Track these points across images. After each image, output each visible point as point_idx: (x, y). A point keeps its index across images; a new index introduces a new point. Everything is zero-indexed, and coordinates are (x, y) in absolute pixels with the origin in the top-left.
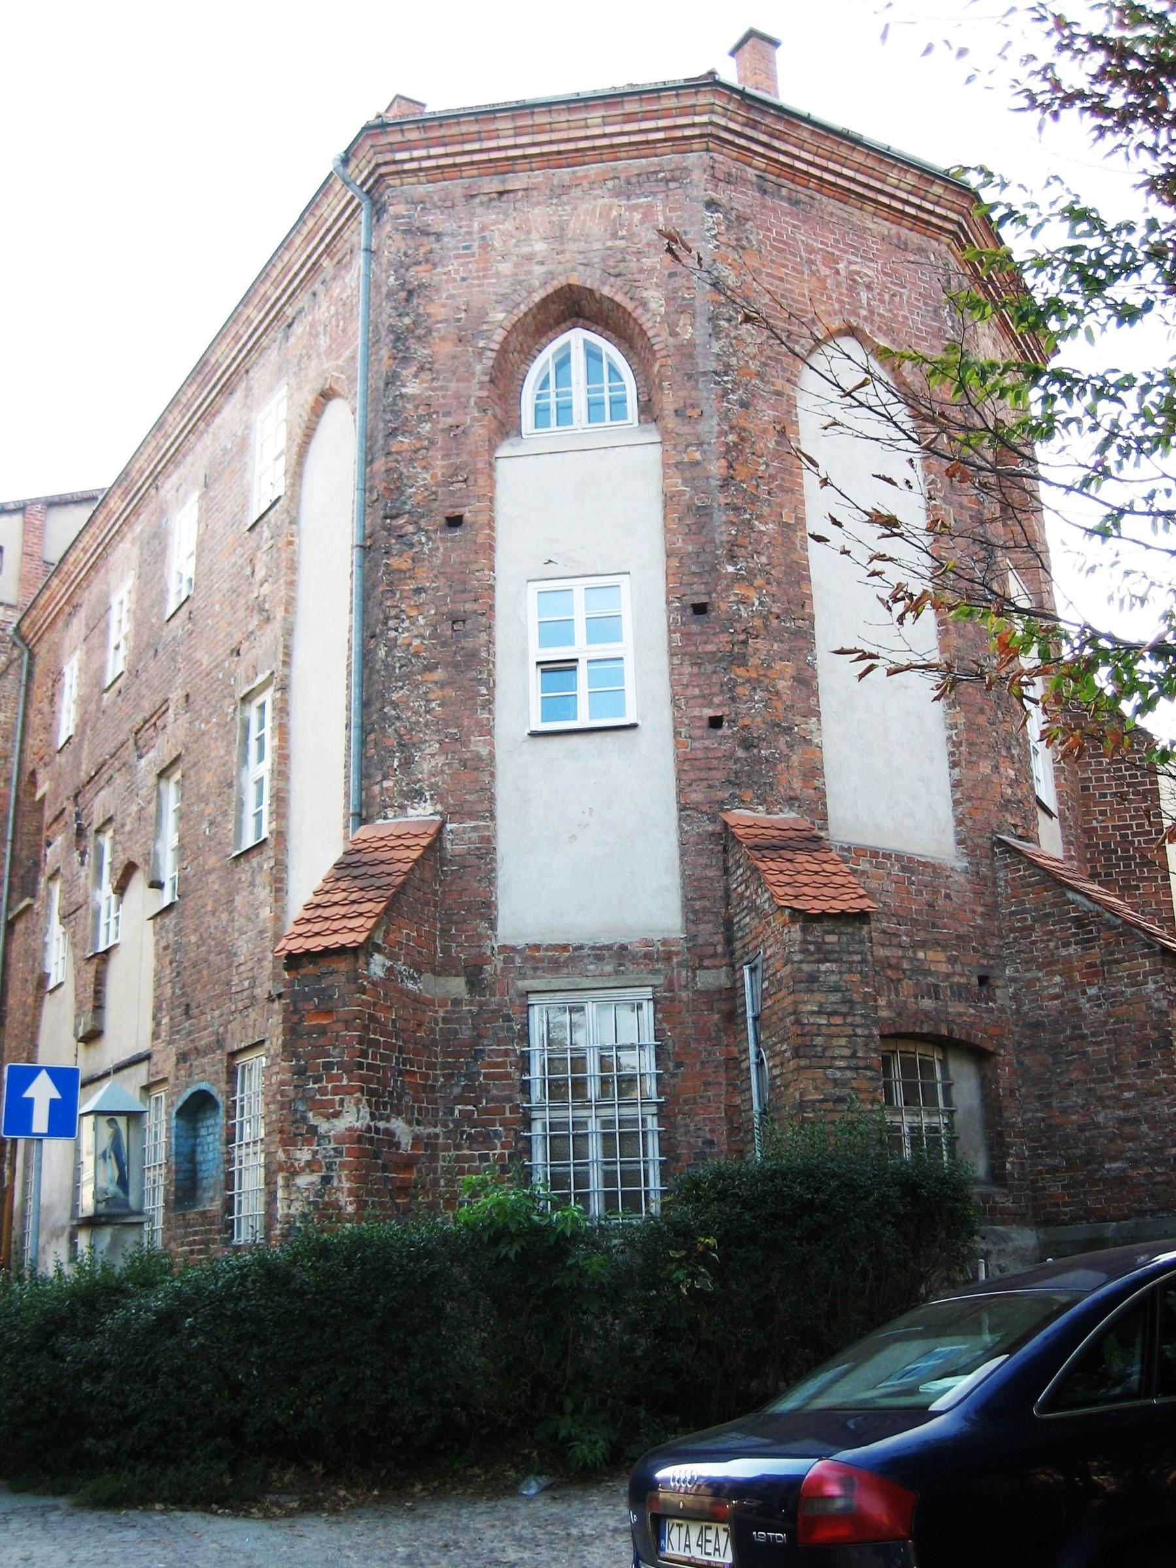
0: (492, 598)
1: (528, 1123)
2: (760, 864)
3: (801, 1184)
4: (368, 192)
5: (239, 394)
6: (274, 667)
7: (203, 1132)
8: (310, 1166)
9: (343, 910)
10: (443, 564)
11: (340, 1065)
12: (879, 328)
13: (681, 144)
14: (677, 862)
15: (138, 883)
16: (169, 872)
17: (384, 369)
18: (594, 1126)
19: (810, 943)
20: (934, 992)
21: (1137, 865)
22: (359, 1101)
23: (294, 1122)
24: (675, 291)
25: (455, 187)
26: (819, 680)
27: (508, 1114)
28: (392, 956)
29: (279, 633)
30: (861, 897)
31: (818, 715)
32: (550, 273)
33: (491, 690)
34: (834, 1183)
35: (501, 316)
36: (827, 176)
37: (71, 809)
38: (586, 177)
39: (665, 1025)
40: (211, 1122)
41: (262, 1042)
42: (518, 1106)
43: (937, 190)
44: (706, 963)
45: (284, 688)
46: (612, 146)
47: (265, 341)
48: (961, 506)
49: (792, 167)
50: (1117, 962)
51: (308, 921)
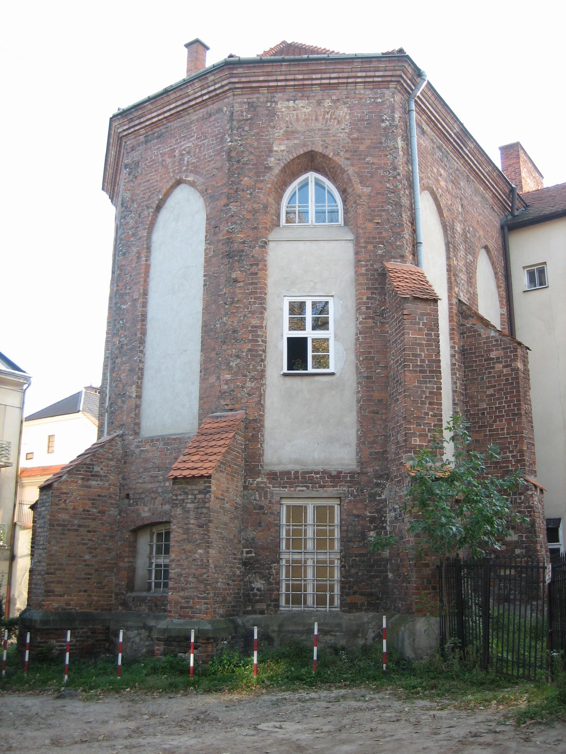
36: (166, 115)
43: (211, 78)
49: (153, 123)
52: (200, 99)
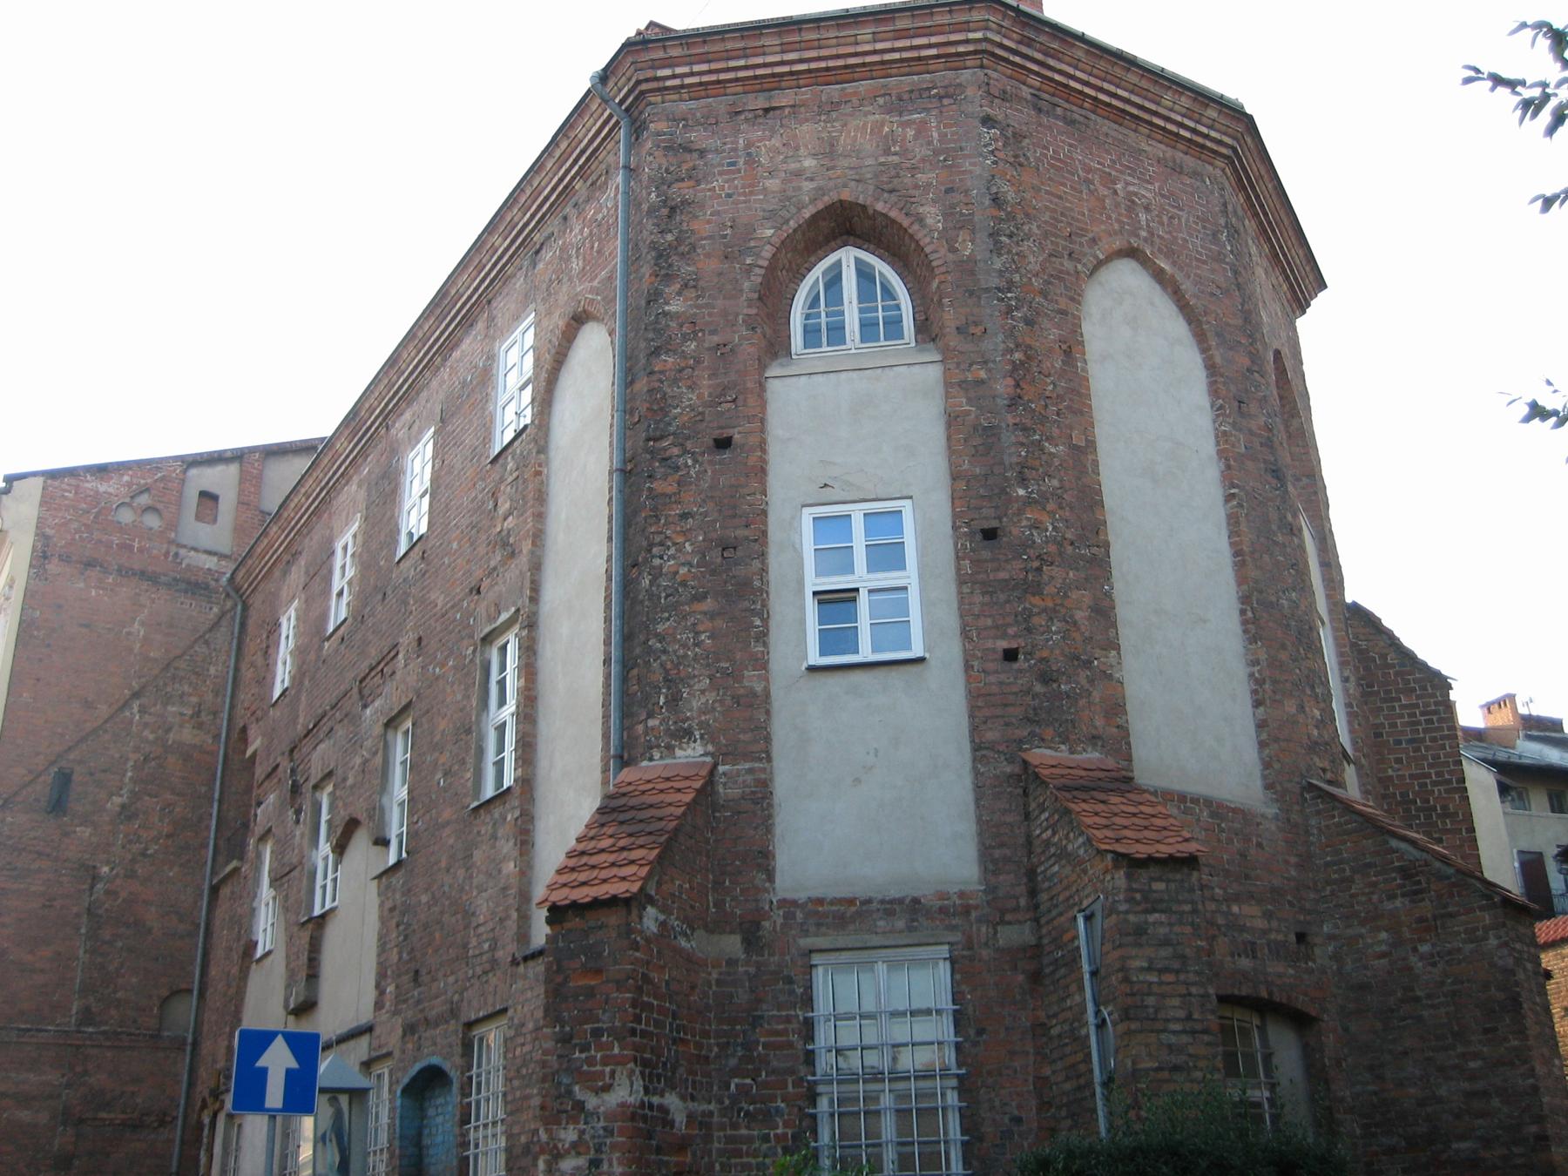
0: (765, 523)
1: (813, 1098)
2: (1072, 806)
3: (1166, 1163)
4: (627, 110)
5: (480, 325)
6: (519, 604)
7: (431, 1112)
8: (577, 1147)
9: (612, 858)
10: (710, 487)
11: (612, 1031)
12: (1160, 250)
13: (953, 60)
14: (972, 807)
15: (360, 843)
16: (396, 827)
17: (645, 287)
18: (887, 1101)
19: (1137, 891)
20: (1251, 950)
21: (1439, 816)
22: (632, 1072)
23: (558, 1097)
24: (953, 206)
25: (720, 105)
26: (1117, 610)
27: (790, 1088)
28: (664, 909)
29: (525, 568)
30: (1187, 840)
31: (1118, 648)
32: (820, 188)
33: (766, 621)
34: (1204, 1164)
35: (769, 232)
36: (1102, 97)
37: (285, 765)
38: (855, 93)
39: (964, 987)
40: (441, 1101)
41: (505, 1010)
42: (802, 1080)
44: (1008, 917)
45: (531, 625)
46: (883, 63)
47: (510, 270)
48: (1251, 432)
49: (1066, 86)
50: (1451, 915)
51: (573, 869)
52: (1173, 128)
